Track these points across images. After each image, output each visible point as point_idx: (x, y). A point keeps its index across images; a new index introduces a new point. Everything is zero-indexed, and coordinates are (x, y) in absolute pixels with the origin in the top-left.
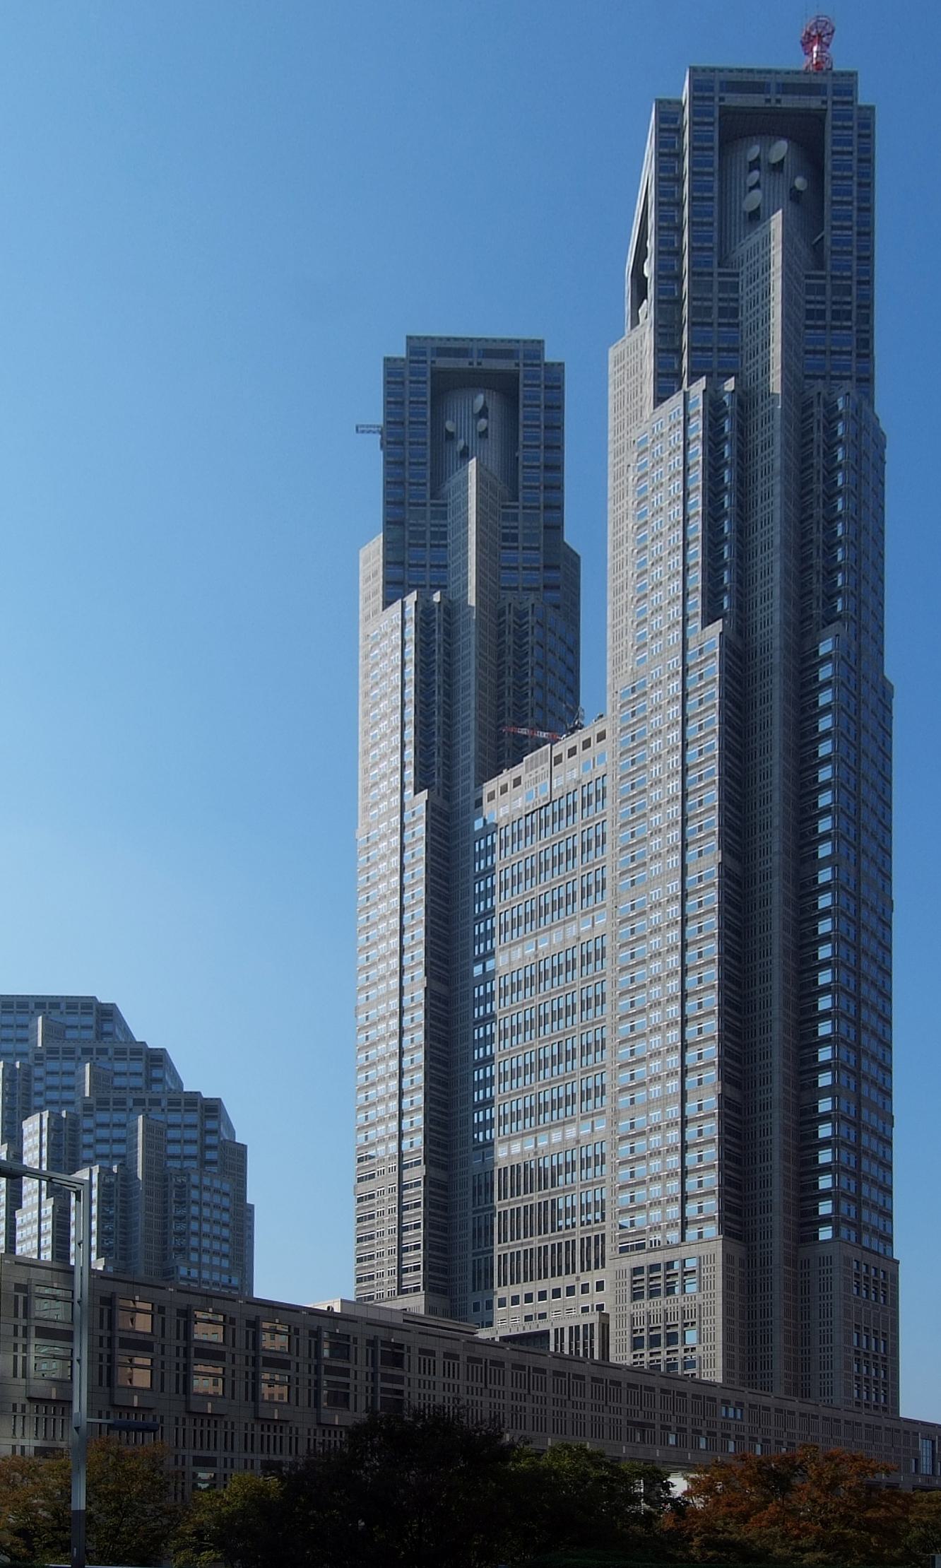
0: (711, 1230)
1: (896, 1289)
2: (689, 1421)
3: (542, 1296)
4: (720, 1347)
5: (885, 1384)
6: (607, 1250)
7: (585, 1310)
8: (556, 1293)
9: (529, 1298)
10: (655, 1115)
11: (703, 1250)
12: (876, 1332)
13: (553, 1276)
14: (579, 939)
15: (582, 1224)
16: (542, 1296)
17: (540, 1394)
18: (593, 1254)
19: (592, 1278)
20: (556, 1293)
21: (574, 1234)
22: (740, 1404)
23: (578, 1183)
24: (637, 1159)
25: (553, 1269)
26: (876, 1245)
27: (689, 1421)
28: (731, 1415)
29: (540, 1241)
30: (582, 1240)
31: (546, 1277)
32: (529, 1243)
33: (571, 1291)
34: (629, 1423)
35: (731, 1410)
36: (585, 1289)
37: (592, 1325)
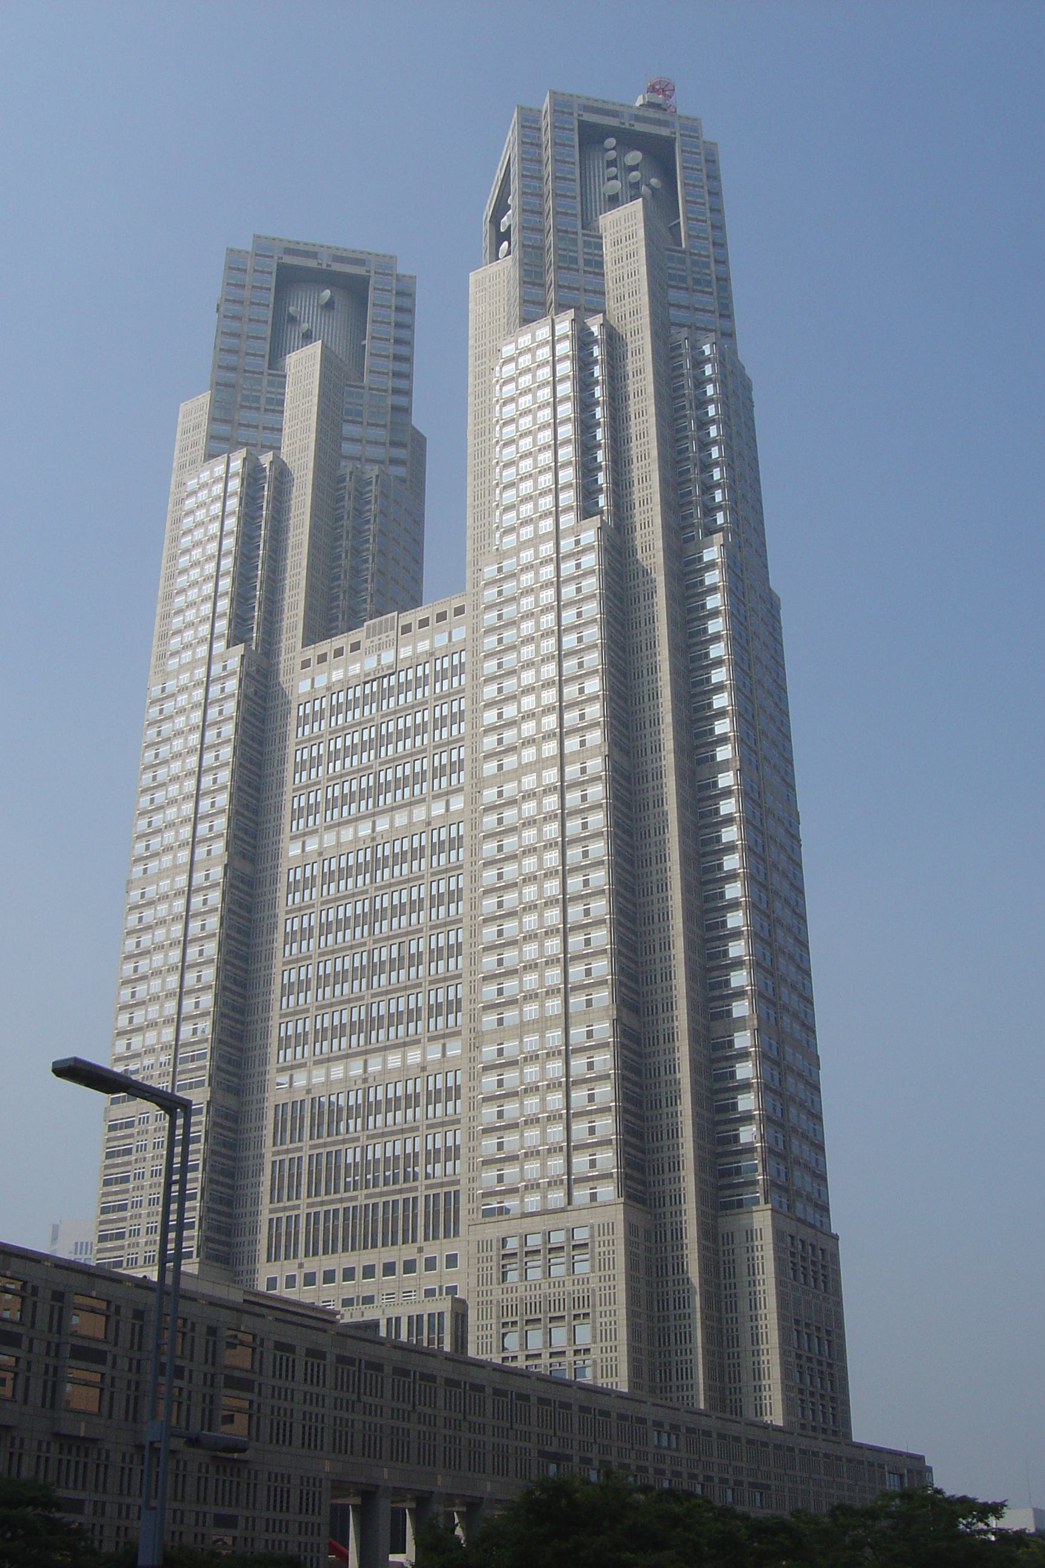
0: (608, 1191)
1: (837, 1272)
2: (614, 1451)
3: (369, 1271)
4: (623, 1349)
5: (833, 1399)
6: (462, 1213)
7: (430, 1293)
8: (389, 1269)
9: (349, 1274)
10: (531, 1041)
11: (598, 1217)
12: (818, 1329)
13: (325, 1252)
14: (429, 824)
15: (427, 1176)
16: (369, 1271)
17: (429, 1411)
18: (444, 1217)
19: (438, 1249)
20: (389, 1269)
21: (415, 1189)
22: (675, 1428)
23: (422, 1124)
24: (506, 1096)
25: (405, 1231)
26: (811, 1216)
27: (614, 1451)
28: (665, 1443)
29: (368, 1197)
30: (427, 1197)
31: (375, 1246)
32: (352, 1199)
33: (410, 1266)
34: (542, 1453)
35: (665, 1436)
36: (430, 1264)
37: (441, 1314)
